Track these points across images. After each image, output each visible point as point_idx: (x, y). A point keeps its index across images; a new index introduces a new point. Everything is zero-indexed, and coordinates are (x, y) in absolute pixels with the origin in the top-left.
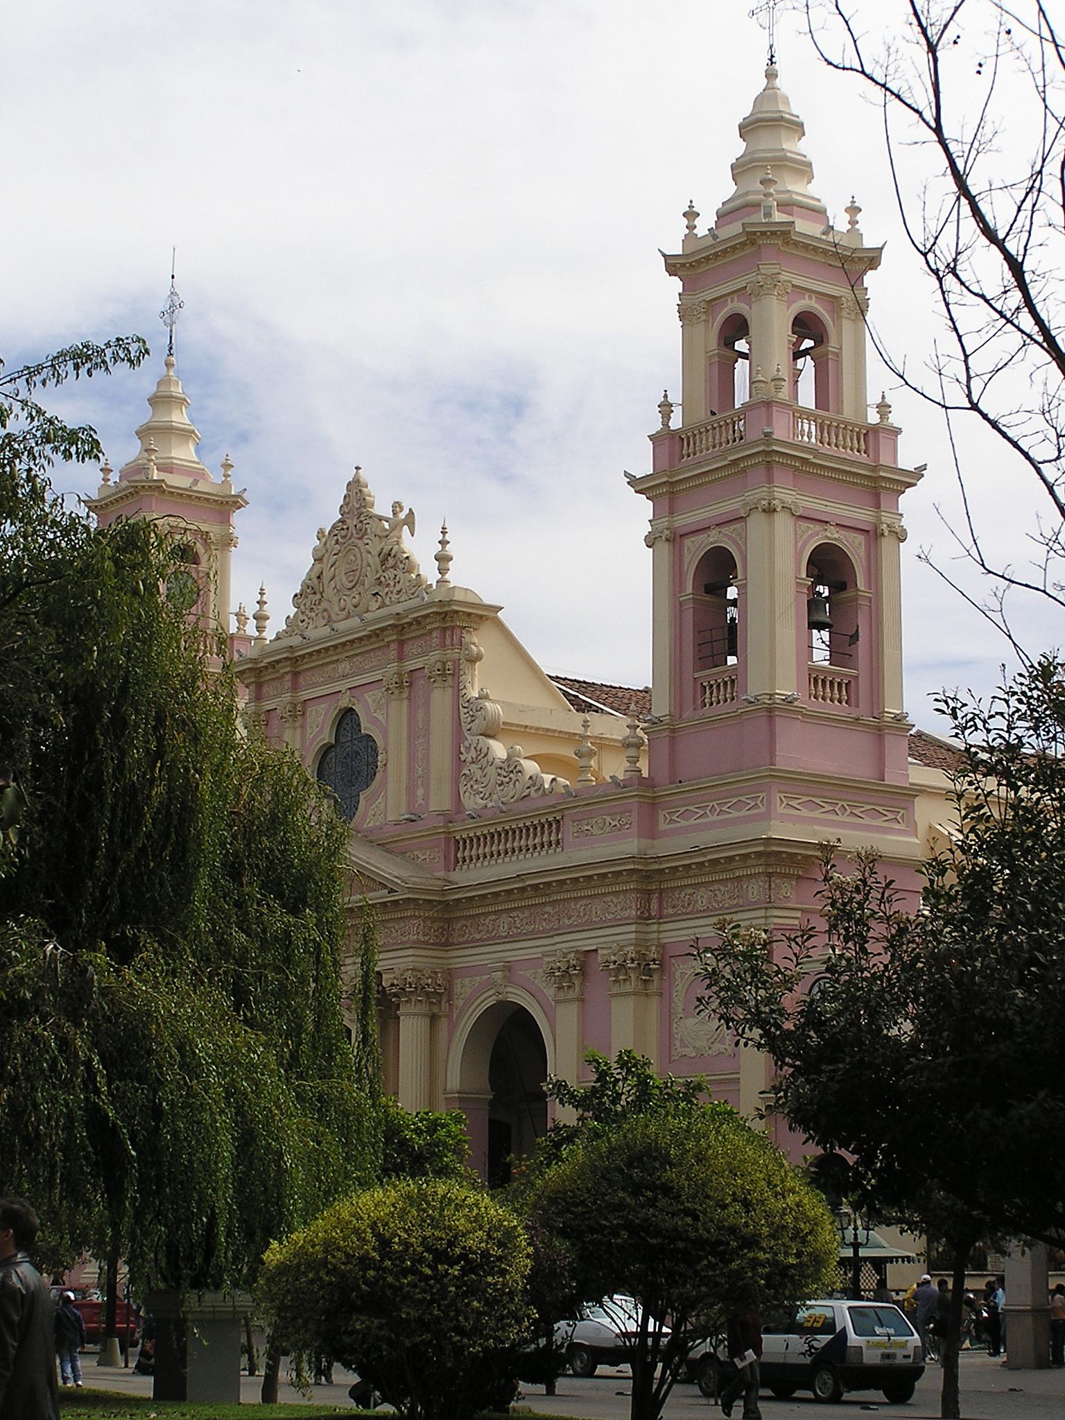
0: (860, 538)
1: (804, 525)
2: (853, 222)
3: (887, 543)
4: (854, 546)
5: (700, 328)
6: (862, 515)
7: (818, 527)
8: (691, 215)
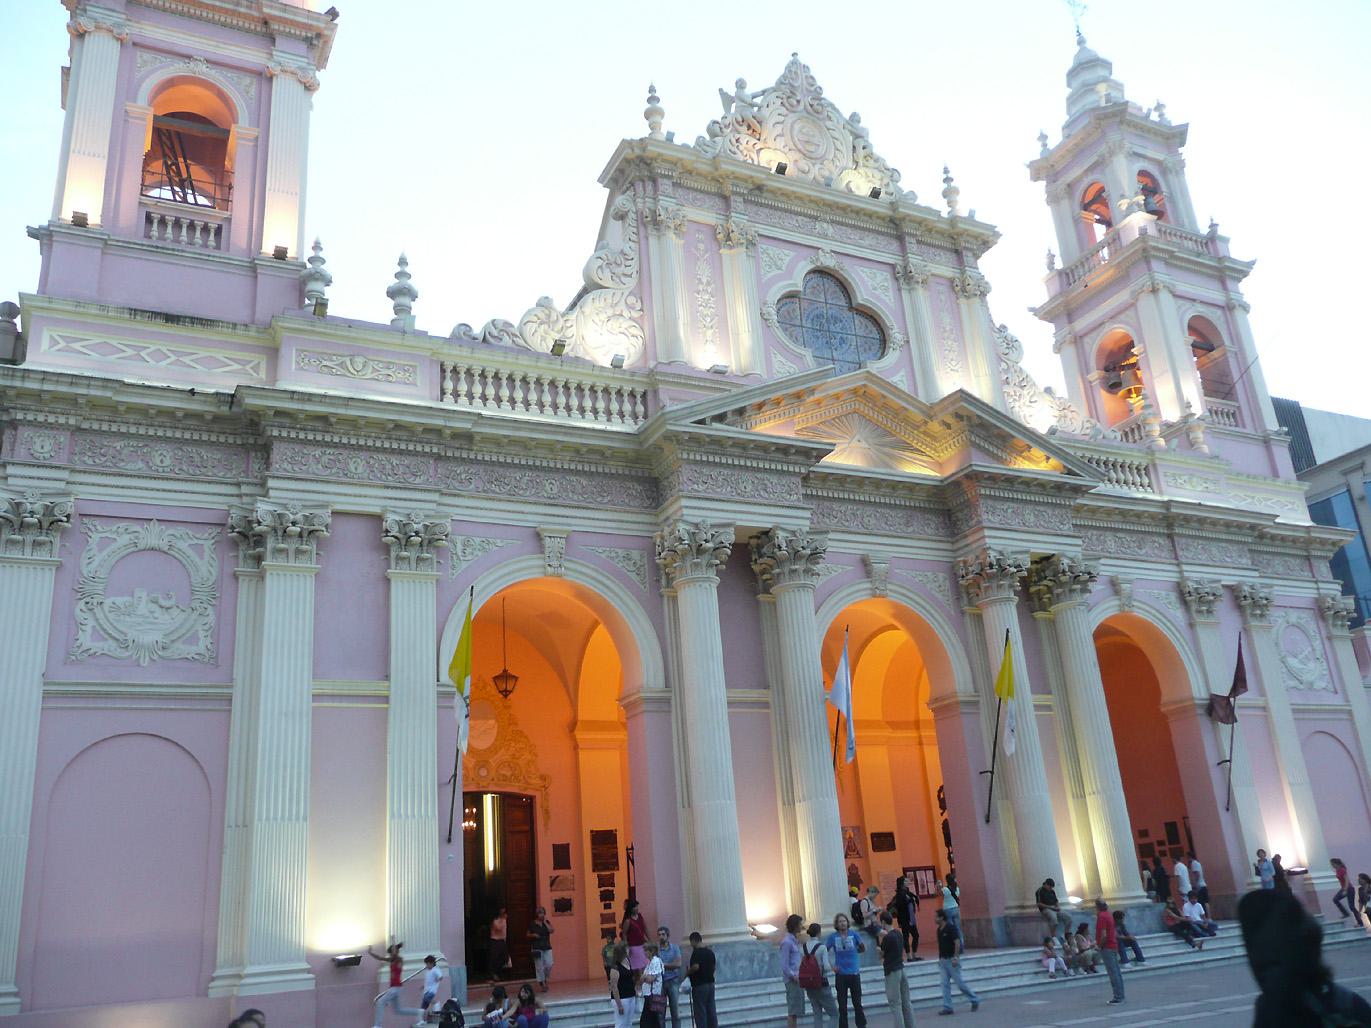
0: (1219, 312)
1: (1181, 302)
2: (1161, 116)
3: (1238, 313)
4: (1215, 316)
5: (1065, 203)
6: (1217, 296)
7: (1188, 304)
8: (1043, 137)
